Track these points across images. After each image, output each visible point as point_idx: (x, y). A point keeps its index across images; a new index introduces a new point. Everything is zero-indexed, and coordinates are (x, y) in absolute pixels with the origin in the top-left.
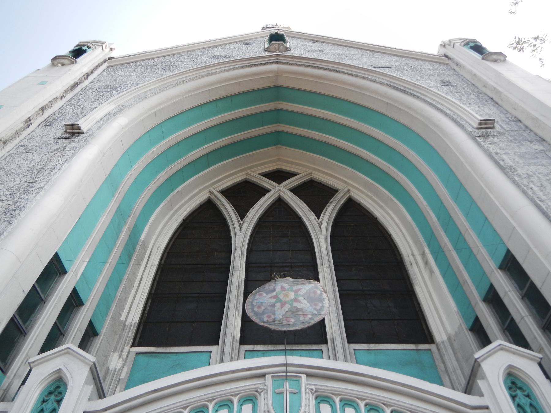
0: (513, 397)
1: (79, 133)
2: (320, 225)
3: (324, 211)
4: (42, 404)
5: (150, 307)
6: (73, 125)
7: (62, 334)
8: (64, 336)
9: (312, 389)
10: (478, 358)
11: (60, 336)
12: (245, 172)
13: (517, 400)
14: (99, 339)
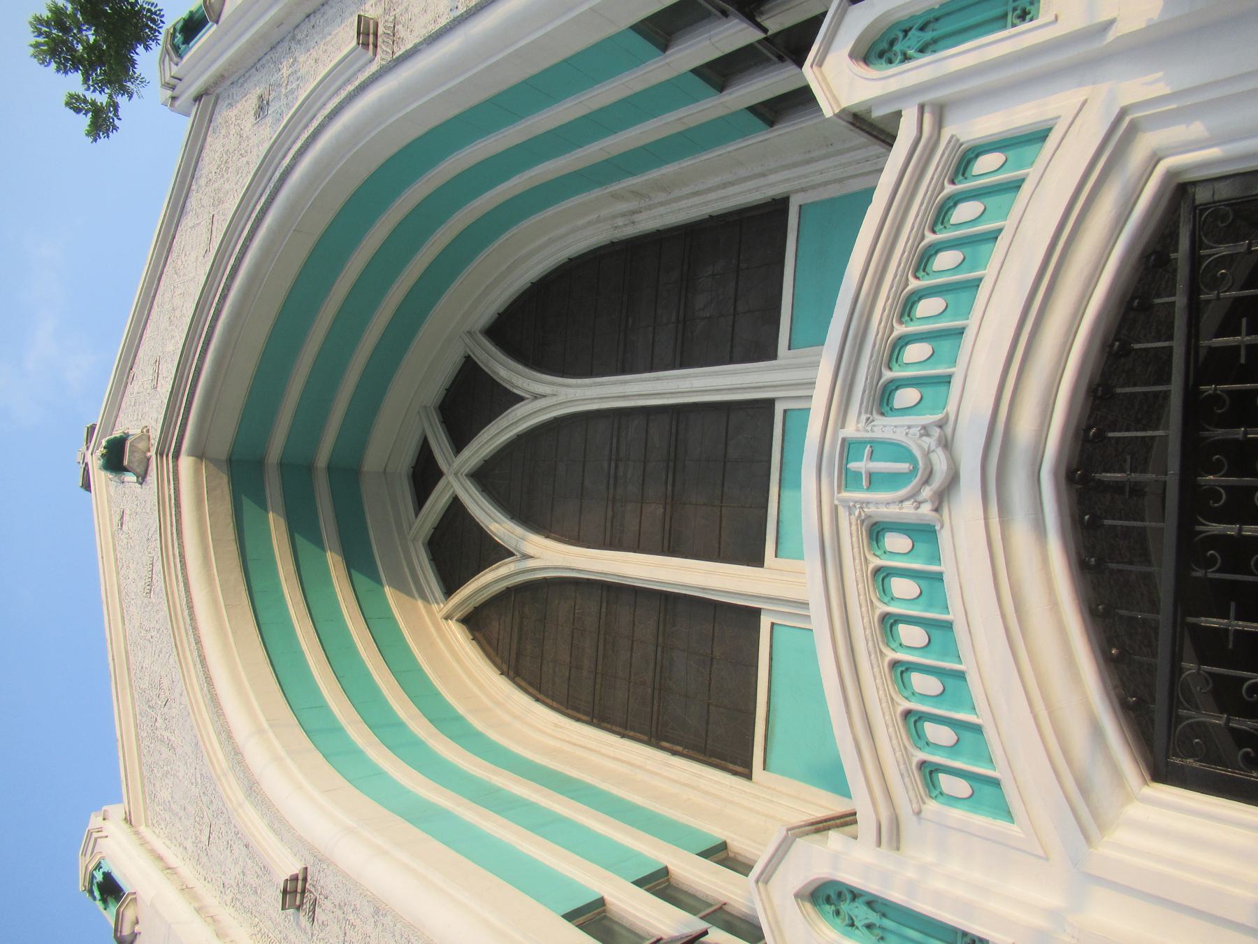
0: (906, 58)
1: (305, 880)
2: (536, 397)
3: (508, 387)
4: (857, 928)
6: (285, 892)
7: (721, 908)
8: (725, 904)
9: (868, 419)
11: (728, 913)
12: (410, 543)
13: (911, 52)
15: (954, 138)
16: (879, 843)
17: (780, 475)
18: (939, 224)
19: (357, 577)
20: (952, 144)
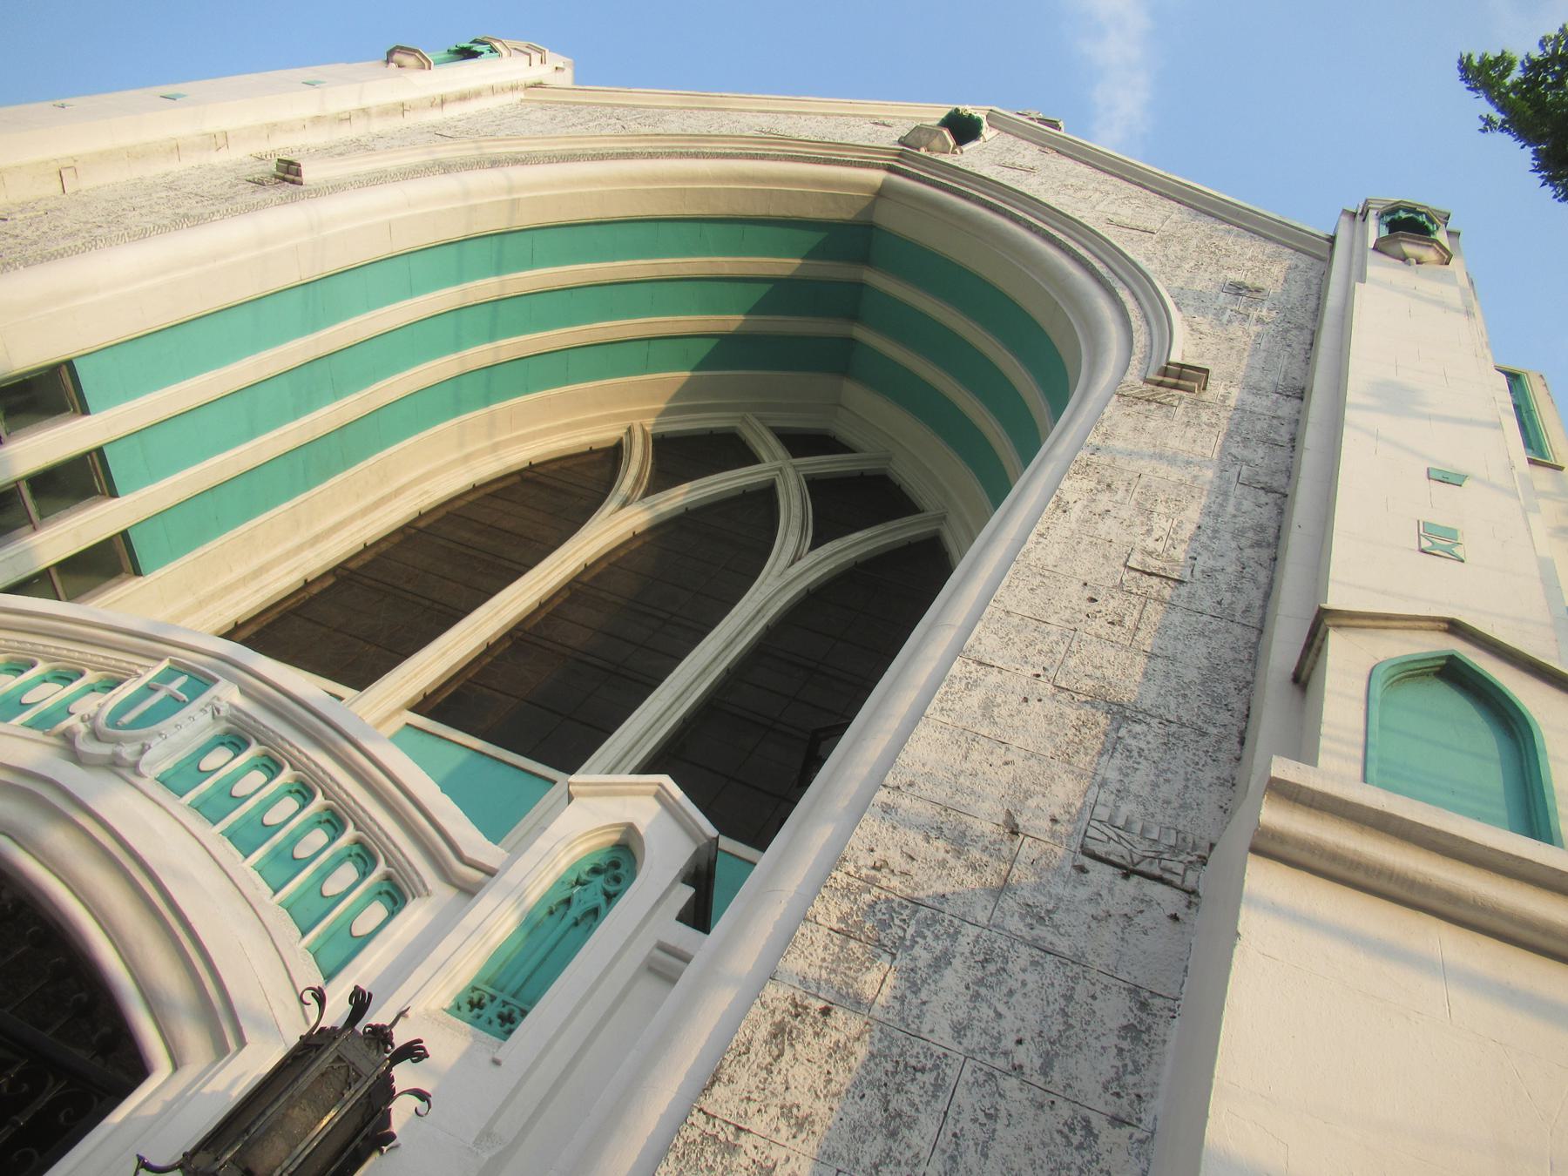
1: (293, 182)
6: (291, 163)
10: (574, 784)
14: (138, 583)
15: (424, 893)
18: (360, 851)
19: (707, 346)
20: (420, 887)
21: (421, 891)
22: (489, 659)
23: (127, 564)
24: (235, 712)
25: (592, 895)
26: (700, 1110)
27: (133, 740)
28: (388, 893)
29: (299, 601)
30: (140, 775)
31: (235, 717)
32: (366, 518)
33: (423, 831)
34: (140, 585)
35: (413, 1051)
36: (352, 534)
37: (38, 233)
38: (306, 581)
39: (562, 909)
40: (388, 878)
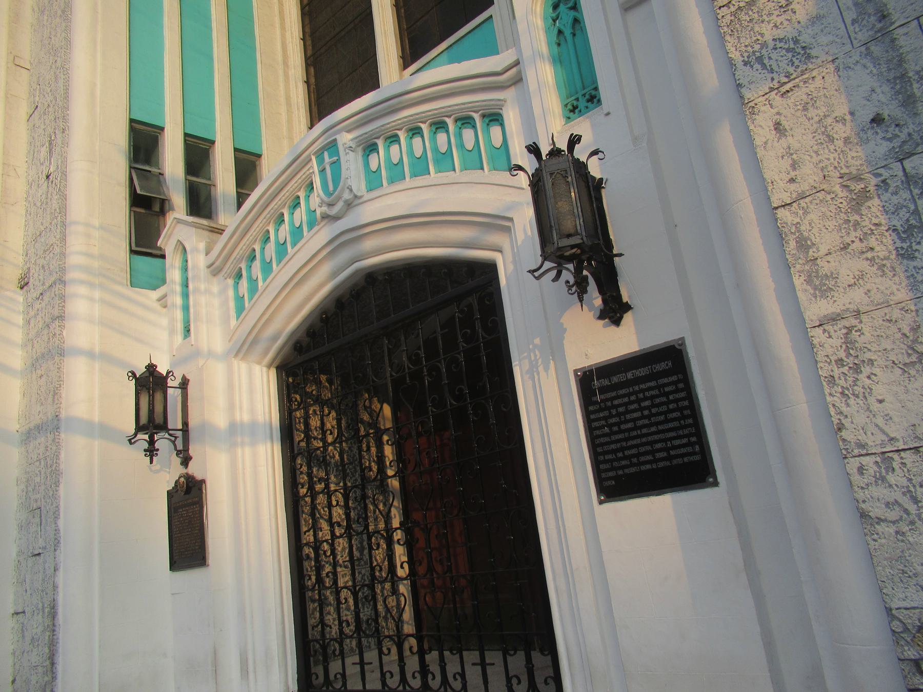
5: (316, 76)
16: (209, 267)
17: (454, 44)
21: (501, 103)
22: (403, 11)
23: (253, 158)
24: (357, 140)
25: (567, 16)
26: (720, 8)
27: (343, 191)
28: (490, 121)
29: (314, 92)
30: (361, 197)
31: (359, 142)
32: (287, 29)
33: (472, 85)
34: (266, 158)
35: (574, 141)
36: (292, 42)
37: (50, 94)
38: (305, 82)
39: (562, 38)
40: (484, 116)
